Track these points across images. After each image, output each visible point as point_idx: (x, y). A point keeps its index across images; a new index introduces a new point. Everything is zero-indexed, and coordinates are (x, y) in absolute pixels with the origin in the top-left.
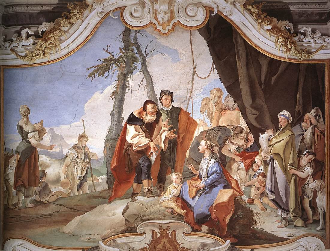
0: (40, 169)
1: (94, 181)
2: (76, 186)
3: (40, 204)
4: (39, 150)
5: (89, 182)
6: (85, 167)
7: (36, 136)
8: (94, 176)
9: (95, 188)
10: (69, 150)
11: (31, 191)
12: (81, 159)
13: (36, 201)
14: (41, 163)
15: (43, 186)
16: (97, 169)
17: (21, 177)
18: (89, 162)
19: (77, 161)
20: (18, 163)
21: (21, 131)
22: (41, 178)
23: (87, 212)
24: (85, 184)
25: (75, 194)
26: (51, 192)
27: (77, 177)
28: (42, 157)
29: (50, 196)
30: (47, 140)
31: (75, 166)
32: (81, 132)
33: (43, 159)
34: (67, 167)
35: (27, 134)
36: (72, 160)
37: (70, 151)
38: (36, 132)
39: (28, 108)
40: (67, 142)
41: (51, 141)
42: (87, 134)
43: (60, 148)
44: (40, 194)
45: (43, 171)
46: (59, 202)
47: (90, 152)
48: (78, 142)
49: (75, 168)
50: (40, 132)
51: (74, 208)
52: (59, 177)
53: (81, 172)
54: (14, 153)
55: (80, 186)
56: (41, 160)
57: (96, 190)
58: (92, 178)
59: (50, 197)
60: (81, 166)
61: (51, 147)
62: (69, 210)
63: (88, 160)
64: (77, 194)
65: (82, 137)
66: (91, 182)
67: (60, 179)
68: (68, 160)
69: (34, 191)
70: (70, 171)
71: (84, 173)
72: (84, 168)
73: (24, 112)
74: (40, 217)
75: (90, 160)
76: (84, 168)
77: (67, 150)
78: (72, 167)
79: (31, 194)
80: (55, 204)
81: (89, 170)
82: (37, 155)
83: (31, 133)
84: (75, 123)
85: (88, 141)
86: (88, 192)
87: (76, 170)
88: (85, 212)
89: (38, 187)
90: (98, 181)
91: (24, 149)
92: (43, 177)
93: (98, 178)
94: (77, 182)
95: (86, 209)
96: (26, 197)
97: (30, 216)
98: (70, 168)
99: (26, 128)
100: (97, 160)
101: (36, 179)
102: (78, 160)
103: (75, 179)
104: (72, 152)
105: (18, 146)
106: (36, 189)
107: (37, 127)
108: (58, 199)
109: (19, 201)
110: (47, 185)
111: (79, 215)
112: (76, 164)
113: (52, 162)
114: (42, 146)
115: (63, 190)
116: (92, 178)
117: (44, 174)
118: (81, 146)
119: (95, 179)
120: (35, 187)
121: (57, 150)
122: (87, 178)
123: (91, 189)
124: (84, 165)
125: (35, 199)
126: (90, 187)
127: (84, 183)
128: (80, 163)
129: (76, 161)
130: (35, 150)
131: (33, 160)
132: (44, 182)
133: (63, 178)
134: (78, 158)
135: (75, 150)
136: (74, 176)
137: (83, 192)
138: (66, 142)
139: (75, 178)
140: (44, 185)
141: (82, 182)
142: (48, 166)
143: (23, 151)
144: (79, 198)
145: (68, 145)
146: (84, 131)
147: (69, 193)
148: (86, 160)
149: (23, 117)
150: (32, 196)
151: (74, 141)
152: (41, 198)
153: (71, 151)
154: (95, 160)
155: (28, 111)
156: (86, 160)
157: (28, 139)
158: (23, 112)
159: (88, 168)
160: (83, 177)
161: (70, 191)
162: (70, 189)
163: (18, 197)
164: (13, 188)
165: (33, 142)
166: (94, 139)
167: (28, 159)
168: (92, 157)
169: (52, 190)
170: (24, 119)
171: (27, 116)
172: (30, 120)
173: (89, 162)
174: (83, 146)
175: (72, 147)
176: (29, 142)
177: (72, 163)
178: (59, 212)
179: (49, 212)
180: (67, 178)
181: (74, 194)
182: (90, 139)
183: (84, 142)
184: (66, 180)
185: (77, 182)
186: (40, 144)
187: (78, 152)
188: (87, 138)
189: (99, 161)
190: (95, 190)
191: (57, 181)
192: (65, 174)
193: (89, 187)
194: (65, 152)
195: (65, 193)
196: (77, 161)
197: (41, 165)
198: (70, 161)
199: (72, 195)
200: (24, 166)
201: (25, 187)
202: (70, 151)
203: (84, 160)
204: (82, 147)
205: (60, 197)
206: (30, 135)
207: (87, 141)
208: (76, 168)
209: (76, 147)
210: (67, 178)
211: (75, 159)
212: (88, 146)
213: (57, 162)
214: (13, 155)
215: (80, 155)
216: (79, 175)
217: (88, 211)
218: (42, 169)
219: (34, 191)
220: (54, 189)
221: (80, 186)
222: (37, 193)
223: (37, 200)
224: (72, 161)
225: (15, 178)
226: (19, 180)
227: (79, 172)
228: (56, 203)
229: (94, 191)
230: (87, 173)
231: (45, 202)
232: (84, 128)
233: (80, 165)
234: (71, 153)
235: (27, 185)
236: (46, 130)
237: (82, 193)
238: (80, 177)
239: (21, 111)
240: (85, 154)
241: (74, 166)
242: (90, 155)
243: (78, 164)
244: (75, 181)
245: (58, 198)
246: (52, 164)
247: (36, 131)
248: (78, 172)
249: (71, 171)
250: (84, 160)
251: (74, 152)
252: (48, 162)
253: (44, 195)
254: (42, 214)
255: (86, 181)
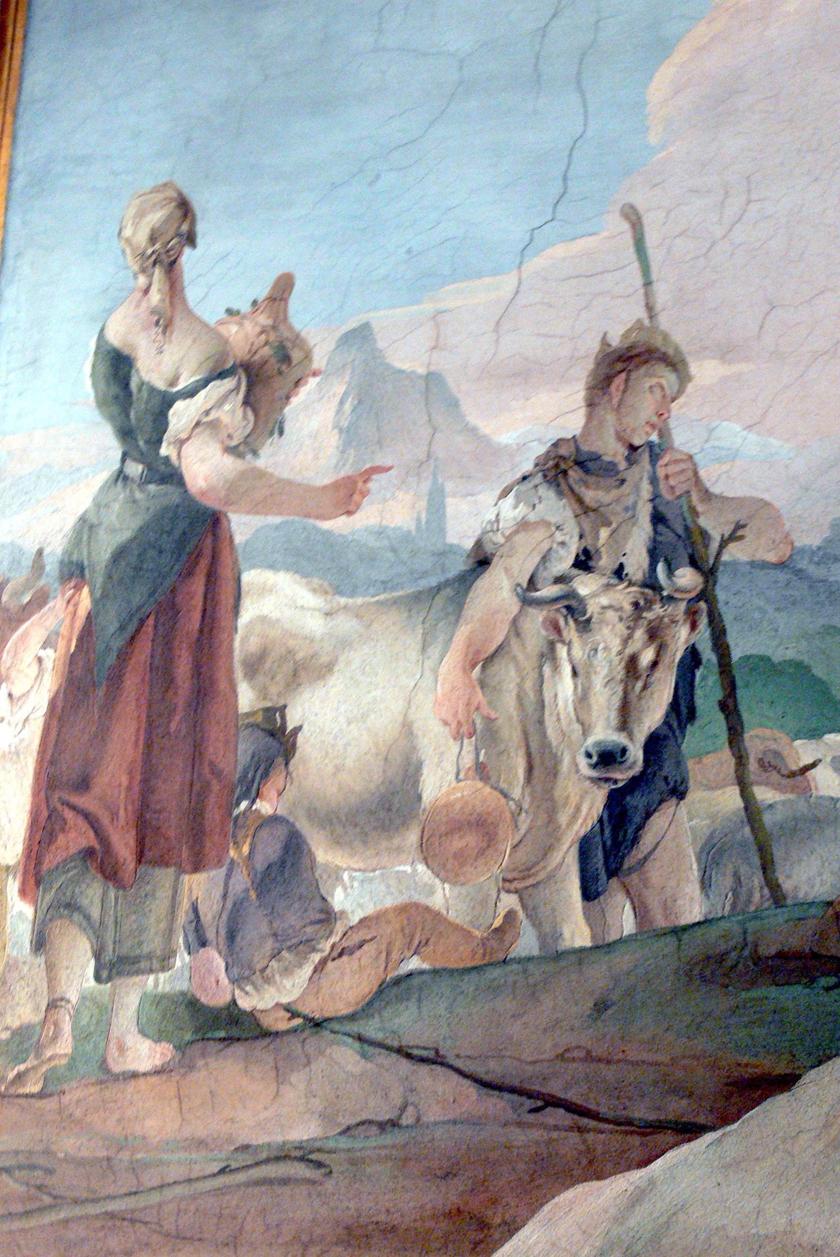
0: (247, 698)
1: (764, 794)
2: (566, 863)
3: (229, 1040)
4: (241, 527)
5: (711, 799)
6: (660, 651)
7: (233, 415)
8: (756, 739)
9: (767, 866)
10: (505, 493)
11: (159, 905)
12: (619, 572)
13: (193, 1004)
14: (254, 645)
15: (260, 865)
16: (790, 654)
17: (83, 784)
18: (706, 595)
19: (583, 591)
20: (72, 659)
21: (115, 389)
22: (251, 789)
23: (689, 1131)
24: (658, 823)
25: (558, 936)
26: (328, 917)
27: (583, 762)
28: (264, 591)
29: (316, 957)
30: (312, 431)
31: (562, 651)
32: (618, 324)
33: (273, 602)
34: (485, 661)
35: (166, 402)
36: (528, 592)
37: (510, 511)
38: (228, 383)
39: (184, 208)
40: (486, 427)
41: (350, 436)
42: (677, 329)
43: (425, 486)
44: (231, 936)
45: (269, 712)
46: (407, 1023)
47: (707, 495)
48: (589, 417)
49: (556, 668)
50: (263, 377)
51: (555, 1088)
52: (407, 761)
53: (616, 701)
54: (51, 566)
55: (612, 851)
56: (263, 619)
57: (787, 885)
58: (741, 760)
59: (323, 962)
60: (615, 644)
61: (348, 494)
62: (497, 1105)
63: (687, 578)
64: (577, 933)
65: (626, 363)
66: (730, 799)
67: (417, 781)
68: (497, 591)
69: (185, 905)
70: (509, 701)
71: (653, 714)
72: (647, 656)
73: (153, 240)
74: (222, 1171)
75: (709, 574)
76: (655, 664)
77: (487, 497)
78: (528, 664)
79: (153, 943)
80: (360, 1039)
81: (708, 690)
82: (225, 572)
83: (191, 393)
84: (559, 251)
85: (690, 388)
86: (692, 907)
87: (565, 688)
88: (668, 1137)
89: (223, 871)
90: (806, 791)
91: (127, 535)
92: (266, 775)
93: (804, 752)
94: (578, 809)
95: (677, 1108)
96: (113, 966)
97: (134, 1168)
98: (508, 676)
99: (153, 368)
100: (781, 565)
101: (206, 788)
102: (585, 586)
103: (561, 782)
104: (532, 517)
105: (83, 520)
106: (202, 888)
107: (241, 338)
108: (393, 989)
109: (53, 1005)
110: (294, 848)
111: (595, 1169)
112: (570, 631)
113: (346, 624)
114: (270, 494)
115: (441, 896)
116: (741, 760)
117: (277, 739)
118: (612, 450)
119: (770, 764)
120: (197, 868)
121: (389, 510)
122: (679, 763)
123: (723, 882)
124: (654, 634)
125: (182, 985)
126: (721, 852)
127: (648, 815)
128: (611, 615)
129: (572, 594)
130: (215, 537)
131: (193, 621)
132: (275, 819)
133: (441, 780)
134: (584, 562)
135: (560, 494)
136: (545, 744)
137: (641, 912)
138: (474, 430)
139: (556, 761)
140: (270, 848)
141: (637, 801)
142: (304, 668)
143: (119, 555)
144: (598, 976)
145: (496, 452)
146: (650, 308)
147: (497, 923)
148: (670, 572)
149: (142, 280)
150: (165, 962)
151: (556, 413)
152: (236, 982)
153: (522, 510)
154: (764, 565)
155: (185, 227)
156: (670, 572)
157: (164, 451)
158: (142, 237)
159: (693, 658)
160: (636, 754)
161: (509, 901)
162: (507, 883)
163: (50, 967)
164: (13, 886)
165: (203, 466)
166: (743, 367)
167: (151, 621)
168: (734, 537)
169: (338, 900)
170: (146, 291)
171: (171, 267)
172: (192, 294)
173: (706, 595)
174: (633, 448)
175: (528, 466)
176: (171, 476)
177: (535, 622)
178: (394, 1124)
179: (305, 1130)
180: (481, 770)
181: (549, 936)
182: (704, 371)
183: (644, 406)
184: (475, 794)
185: (583, 805)
186: (261, 474)
187: (584, 509)
188: (674, 363)
189: (799, 573)
190: (773, 886)
191: (386, 809)
192: (458, 736)
193: (712, 855)
194: (464, 525)
195: (457, 928)
196: (581, 600)
197: (253, 666)
198: (514, 606)
199: (526, 943)
200: (116, 678)
201: (110, 873)
202: (510, 511)
203: (651, 584)
204: (623, 451)
205: (414, 964)
206: (182, 415)
207: (680, 392)
208: (567, 670)
209: (566, 468)
210: (481, 770)
211: (560, 580)
212: (684, 437)
213: (393, 619)
214: (41, 600)
215: (604, 533)
216: (604, 733)
217: (701, 1120)
218: (263, 693)
219: (185, 905)
220: (358, 887)
221: (612, 851)
222: (210, 935)
223: (204, 1000)
224: (527, 602)
225: (36, 794)
226: (69, 815)
227: (604, 700)
228: (371, 1028)
229: (759, 896)
230: (682, 710)
231: (267, 1022)
232: (648, 284)
233: (610, 639)
234: (523, 525)
235: (124, 846)
236: (308, 356)
237: (628, 923)
238: (608, 758)
239: (128, 232)
240: (658, 519)
241: (552, 645)
242: (714, 525)
243: (585, 626)
244: (558, 793)
245: (398, 981)
246: (344, 643)
247: (222, 375)
248: (585, 698)
249: (520, 699)
250: (651, 584)
251: (553, 507)
252: (315, 625)
253: (269, 945)
254: (245, 1148)
255: (678, 792)
